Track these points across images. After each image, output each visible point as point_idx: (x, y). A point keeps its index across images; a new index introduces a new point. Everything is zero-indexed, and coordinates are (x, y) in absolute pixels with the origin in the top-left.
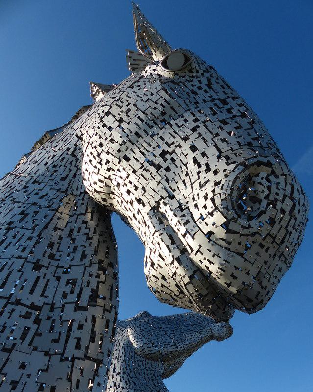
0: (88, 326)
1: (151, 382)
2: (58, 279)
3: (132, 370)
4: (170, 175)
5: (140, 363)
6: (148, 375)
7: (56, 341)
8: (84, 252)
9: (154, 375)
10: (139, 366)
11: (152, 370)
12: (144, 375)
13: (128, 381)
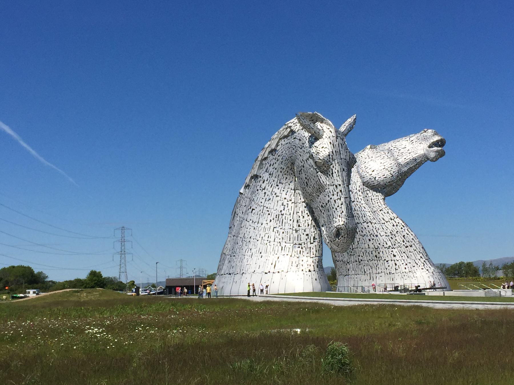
0: (314, 249)
1: (377, 204)
2: (303, 234)
3: (362, 199)
4: (324, 215)
5: (368, 192)
6: (374, 200)
7: (308, 253)
8: (308, 223)
9: (378, 199)
10: (367, 194)
11: (377, 196)
12: (372, 199)
13: (360, 207)
